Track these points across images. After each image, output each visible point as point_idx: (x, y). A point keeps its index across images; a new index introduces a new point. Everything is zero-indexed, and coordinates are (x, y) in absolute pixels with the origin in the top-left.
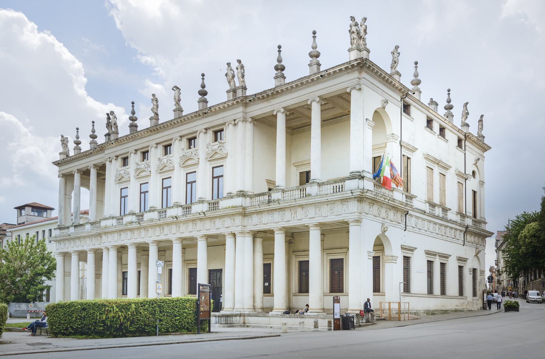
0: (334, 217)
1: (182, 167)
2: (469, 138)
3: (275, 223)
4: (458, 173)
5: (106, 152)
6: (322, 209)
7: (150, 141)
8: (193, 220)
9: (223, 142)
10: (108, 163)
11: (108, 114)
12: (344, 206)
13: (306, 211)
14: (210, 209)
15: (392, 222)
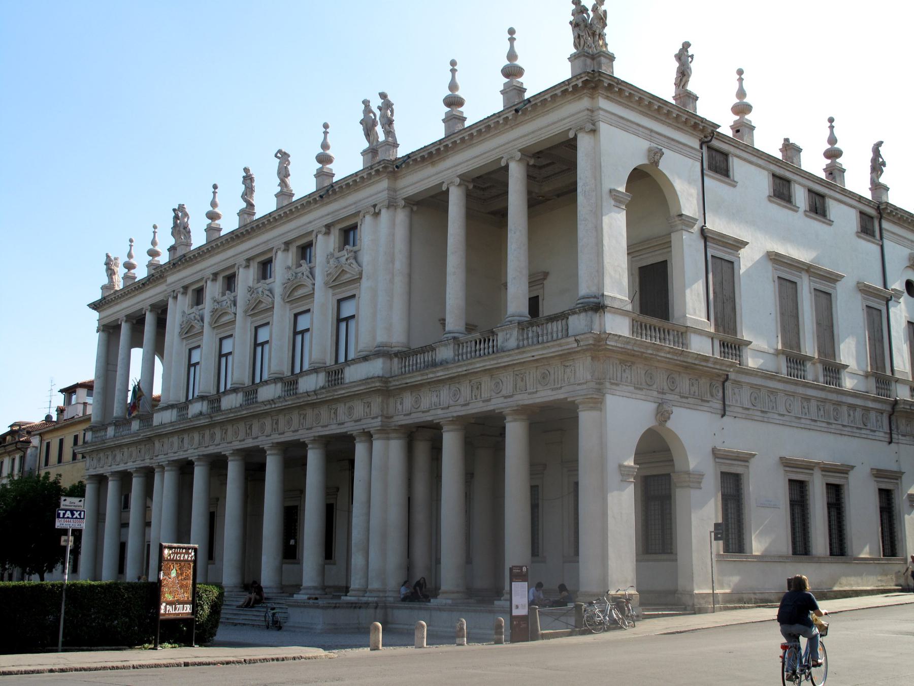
0: (550, 393)
1: (288, 302)
2: (888, 213)
3: (442, 409)
4: (863, 288)
5: (171, 279)
6: (527, 378)
8: (300, 407)
9: (355, 248)
10: (171, 301)
11: (174, 210)
12: (568, 370)
13: (498, 383)
14: (330, 384)
15: (684, 400)
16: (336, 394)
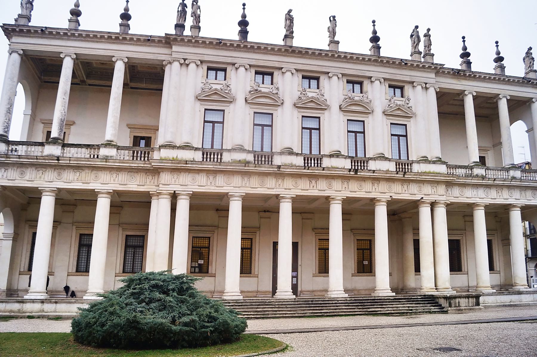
7: (283, 62)
16: (421, 177)
